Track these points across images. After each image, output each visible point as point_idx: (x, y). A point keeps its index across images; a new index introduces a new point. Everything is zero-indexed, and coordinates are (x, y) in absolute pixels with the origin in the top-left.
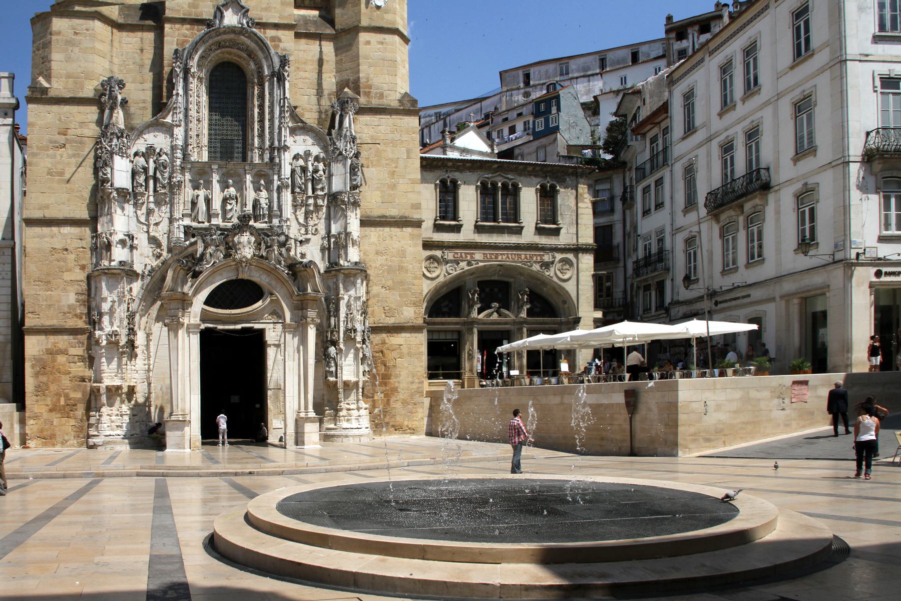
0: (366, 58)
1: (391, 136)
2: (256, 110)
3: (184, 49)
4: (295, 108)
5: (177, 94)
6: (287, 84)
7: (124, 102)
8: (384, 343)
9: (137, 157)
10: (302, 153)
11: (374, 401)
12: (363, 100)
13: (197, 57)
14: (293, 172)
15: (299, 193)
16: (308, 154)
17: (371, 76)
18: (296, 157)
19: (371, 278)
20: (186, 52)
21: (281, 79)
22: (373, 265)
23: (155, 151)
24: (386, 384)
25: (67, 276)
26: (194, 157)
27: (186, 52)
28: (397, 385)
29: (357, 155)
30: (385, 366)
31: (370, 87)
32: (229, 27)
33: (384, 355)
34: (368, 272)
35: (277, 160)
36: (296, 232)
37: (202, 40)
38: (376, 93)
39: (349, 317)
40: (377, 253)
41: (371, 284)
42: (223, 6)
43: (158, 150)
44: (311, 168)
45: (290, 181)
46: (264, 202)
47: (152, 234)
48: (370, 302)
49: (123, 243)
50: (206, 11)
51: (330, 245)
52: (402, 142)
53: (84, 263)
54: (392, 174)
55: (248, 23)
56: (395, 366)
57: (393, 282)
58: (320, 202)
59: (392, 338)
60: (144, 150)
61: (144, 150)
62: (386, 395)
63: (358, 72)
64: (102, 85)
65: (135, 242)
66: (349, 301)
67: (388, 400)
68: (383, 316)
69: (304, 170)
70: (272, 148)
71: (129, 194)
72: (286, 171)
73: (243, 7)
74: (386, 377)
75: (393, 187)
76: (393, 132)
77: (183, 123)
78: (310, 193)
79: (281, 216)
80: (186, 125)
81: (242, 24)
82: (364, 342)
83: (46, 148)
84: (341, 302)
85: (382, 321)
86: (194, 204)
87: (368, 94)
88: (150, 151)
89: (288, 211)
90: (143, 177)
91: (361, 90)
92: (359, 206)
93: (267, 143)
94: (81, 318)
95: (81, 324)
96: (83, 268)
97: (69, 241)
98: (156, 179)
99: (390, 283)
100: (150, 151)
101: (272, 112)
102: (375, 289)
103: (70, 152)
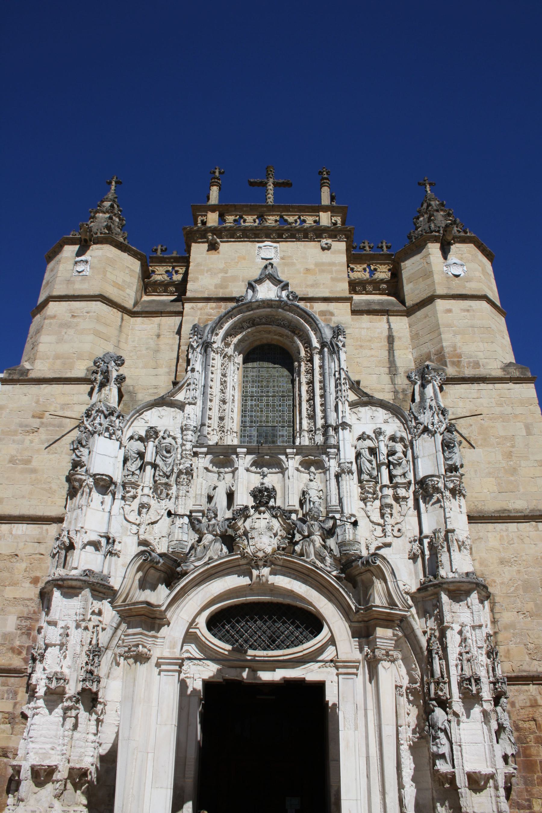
0: (449, 326)
1: (498, 410)
2: (304, 388)
3: (206, 326)
4: (358, 383)
5: (193, 370)
6: (343, 356)
7: (121, 379)
9: (132, 441)
12: (451, 371)
13: (222, 332)
14: (358, 455)
15: (367, 481)
16: (378, 433)
17: (459, 345)
18: (362, 437)
19: (497, 599)
20: (208, 328)
21: (334, 350)
22: (498, 580)
23: (156, 433)
25: (10, 593)
26: (213, 440)
27: (208, 328)
29: (450, 429)
31: (460, 356)
32: (263, 301)
34: (490, 590)
35: (332, 441)
36: (367, 534)
37: (228, 315)
38: (469, 363)
39: (465, 657)
40: (502, 563)
41: (497, 608)
42: (256, 281)
43: (161, 434)
44: (384, 450)
45: (354, 467)
46: (313, 495)
47: (142, 537)
48: (500, 637)
49: (96, 545)
50: (238, 289)
51: (423, 553)
52: (516, 416)
53: (38, 574)
54: (509, 455)
55: (288, 296)
57: (536, 605)
58: (402, 492)
60: (143, 434)
61: (143, 434)
63: (441, 341)
64: (95, 363)
65: (117, 547)
66: (460, 633)
70: (326, 427)
71: (115, 484)
72: (348, 454)
73: (280, 282)
75: (514, 471)
76: (501, 405)
77: (199, 402)
78: (385, 480)
79: (342, 512)
80: (204, 403)
81: (280, 297)
82: (497, 701)
83: (15, 433)
84: (449, 633)
86: (210, 498)
87: (457, 364)
88: (152, 433)
89: (353, 505)
90: (139, 463)
91: (448, 360)
92: (464, 496)
93: (320, 423)
94: (20, 653)
95: (17, 662)
96: (35, 581)
97: (21, 545)
98: (155, 466)
99: (530, 606)
100: (152, 433)
101: (323, 388)
102: (506, 617)
103: (44, 437)
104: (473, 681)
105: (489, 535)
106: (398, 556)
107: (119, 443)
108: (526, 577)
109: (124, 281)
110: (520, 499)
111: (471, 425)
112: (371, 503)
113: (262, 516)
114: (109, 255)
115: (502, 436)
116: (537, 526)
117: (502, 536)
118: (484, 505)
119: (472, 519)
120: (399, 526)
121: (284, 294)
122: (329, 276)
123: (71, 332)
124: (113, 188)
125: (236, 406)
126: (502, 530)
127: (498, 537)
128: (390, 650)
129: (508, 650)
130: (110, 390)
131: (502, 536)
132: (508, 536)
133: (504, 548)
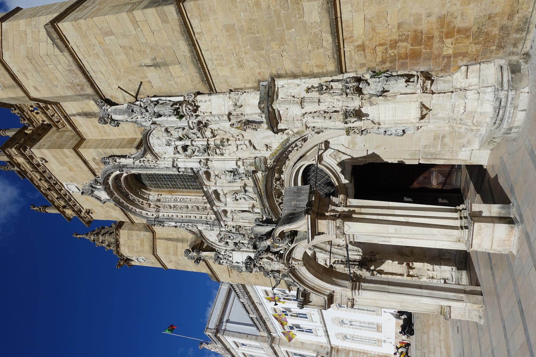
8: (362, 48)
10: (171, 149)
11: (456, 55)
19: (274, 72)
24: (431, 38)
28: (433, 19)
30: (399, 40)
33: (381, 45)
34: (267, 77)
41: (282, 72)
48: (307, 71)
52: (100, 43)
56: (400, 26)
59: (356, 34)
62: (449, 35)
67: (459, 31)
68: (321, 50)
69: (185, 148)
74: (418, 38)
85: (329, 53)
102: (289, 66)
104: (347, 120)
105: (220, 74)
106: (257, 136)
107: (233, 252)
108: (248, 47)
109: (137, 240)
110: (179, 46)
111: (130, 80)
112: (224, 150)
113: (262, 263)
114: (127, 250)
115: (127, 56)
116: (197, 33)
117: (218, 64)
118: (196, 76)
119: (212, 91)
120: (234, 135)
121: (98, 187)
122: (67, 160)
123: (180, 262)
124: (81, 236)
125: (186, 197)
126: (213, 64)
127: (220, 68)
128: (336, 225)
129: (317, 66)
130: (206, 256)
131: (218, 64)
132: (216, 60)
133: (228, 64)
